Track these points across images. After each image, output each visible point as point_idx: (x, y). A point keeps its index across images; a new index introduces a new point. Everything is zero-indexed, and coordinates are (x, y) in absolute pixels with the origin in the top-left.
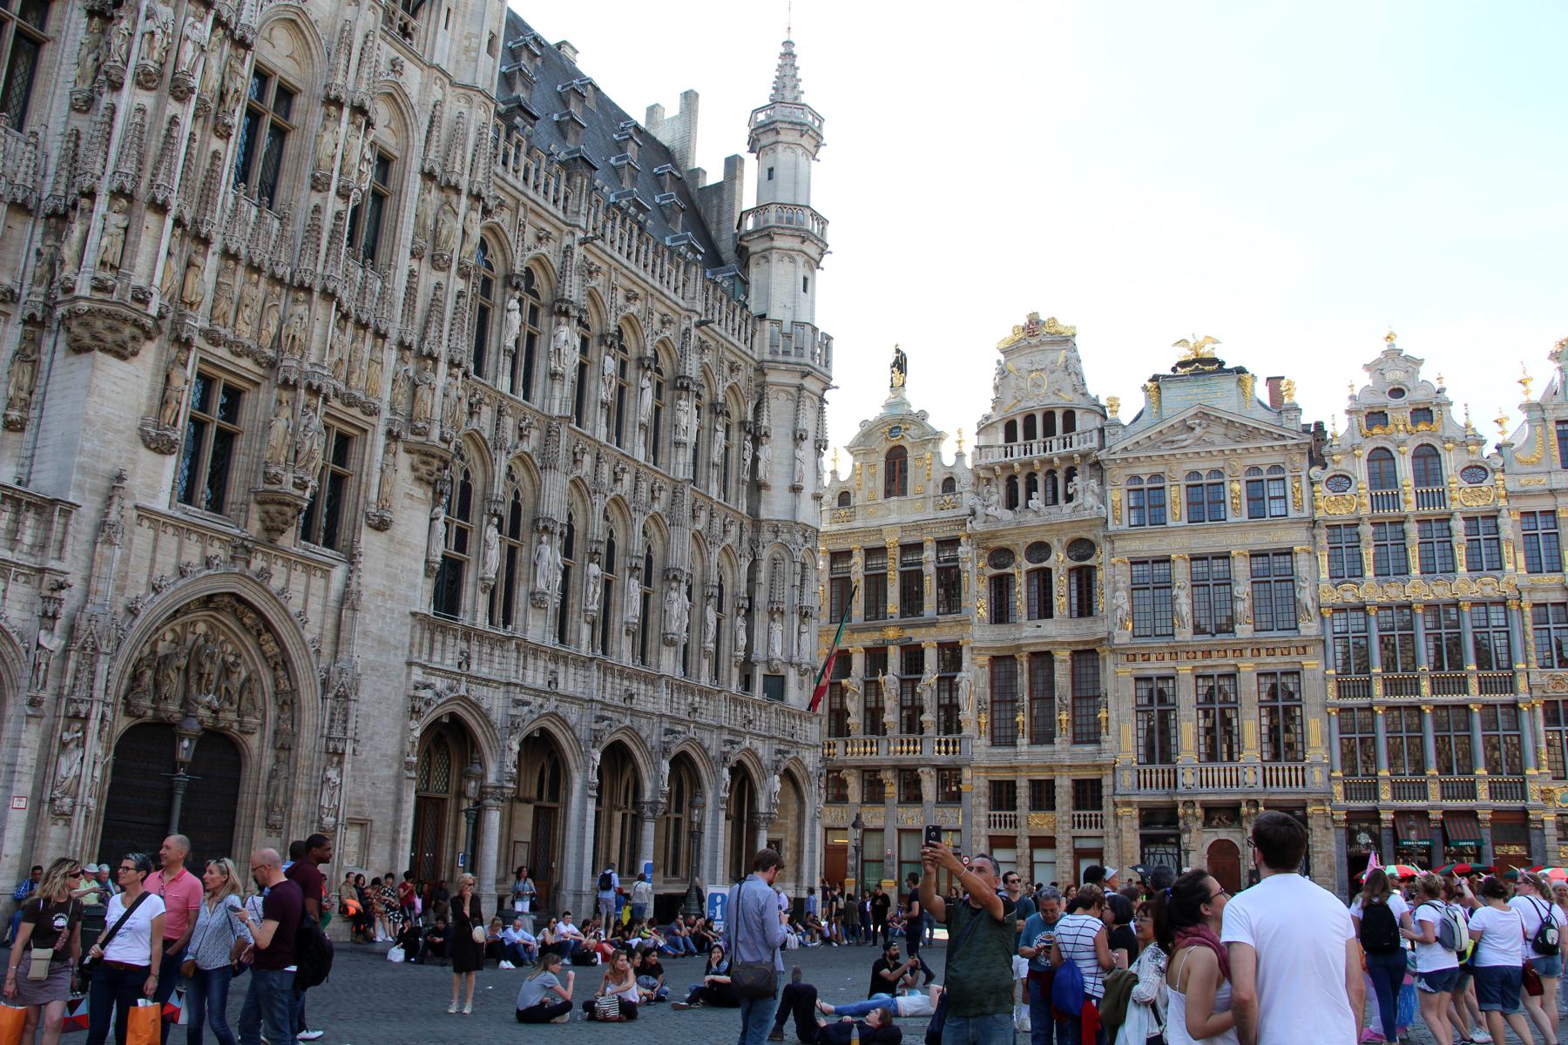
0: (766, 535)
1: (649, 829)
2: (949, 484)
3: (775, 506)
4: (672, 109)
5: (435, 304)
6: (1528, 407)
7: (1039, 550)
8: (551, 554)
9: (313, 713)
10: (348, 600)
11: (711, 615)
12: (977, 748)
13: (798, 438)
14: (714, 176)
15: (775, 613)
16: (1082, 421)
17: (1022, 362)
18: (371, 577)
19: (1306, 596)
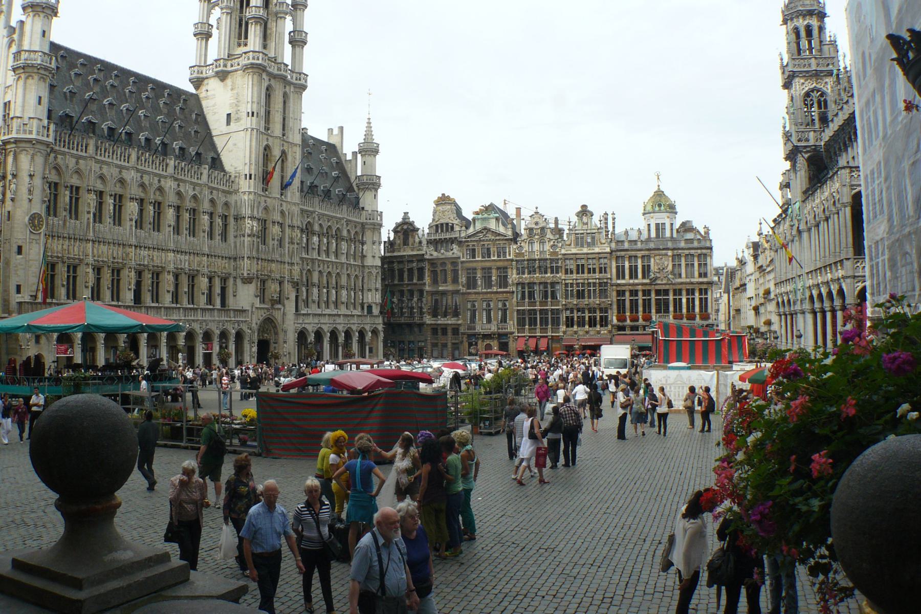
0: (367, 271)
1: (340, 348)
2: (420, 242)
3: (369, 262)
4: (336, 132)
5: (293, 252)
6: (569, 230)
7: (443, 264)
8: (315, 290)
9: (281, 335)
10: (284, 314)
11: (352, 293)
12: (428, 320)
13: (374, 243)
14: (349, 157)
15: (370, 290)
16: (457, 228)
17: (440, 208)
18: (287, 308)
19: (510, 281)
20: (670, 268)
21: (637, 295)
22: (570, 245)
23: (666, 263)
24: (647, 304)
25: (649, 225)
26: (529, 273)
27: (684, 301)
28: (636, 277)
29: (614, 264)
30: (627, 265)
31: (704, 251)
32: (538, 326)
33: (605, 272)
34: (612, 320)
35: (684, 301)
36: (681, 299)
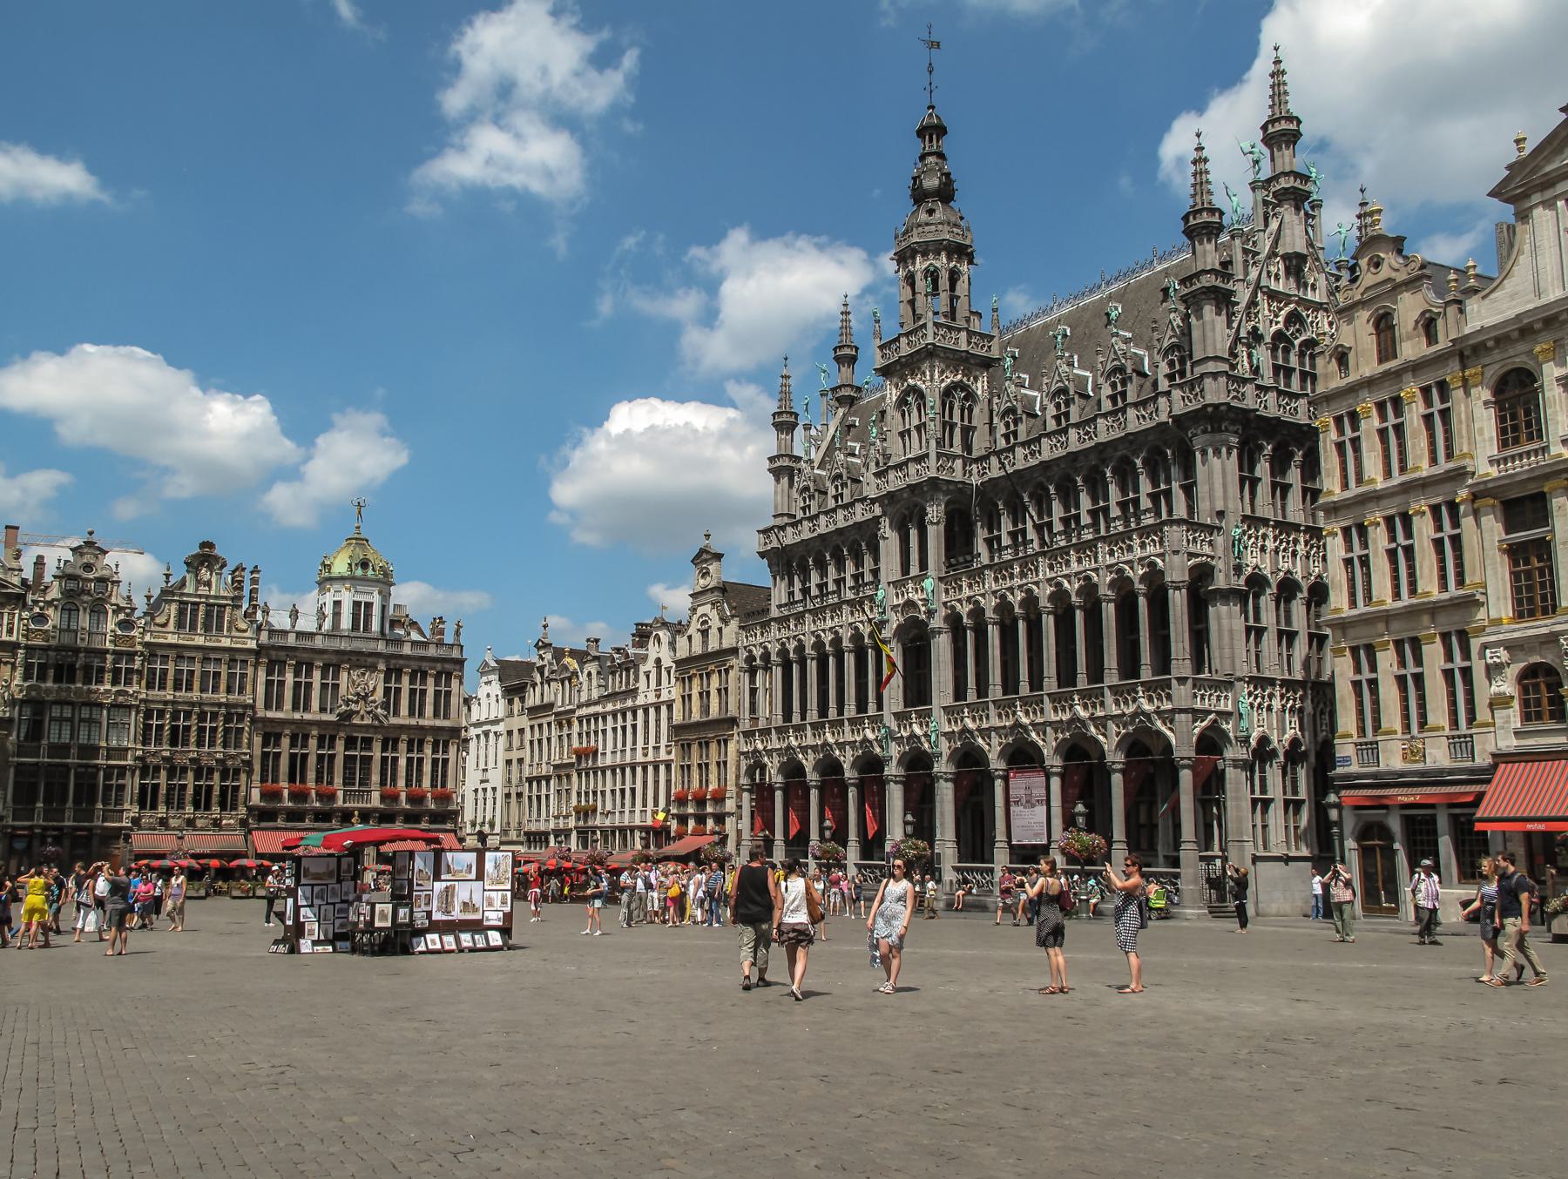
20: (379, 695)
21: (305, 746)
22: (165, 625)
23: (371, 684)
24: (324, 763)
25: (337, 604)
26: (57, 679)
27: (402, 762)
28: (307, 708)
29: (262, 676)
30: (289, 678)
31: (448, 666)
32: (70, 804)
33: (242, 690)
34: (248, 797)
35: (402, 762)
36: (395, 760)
